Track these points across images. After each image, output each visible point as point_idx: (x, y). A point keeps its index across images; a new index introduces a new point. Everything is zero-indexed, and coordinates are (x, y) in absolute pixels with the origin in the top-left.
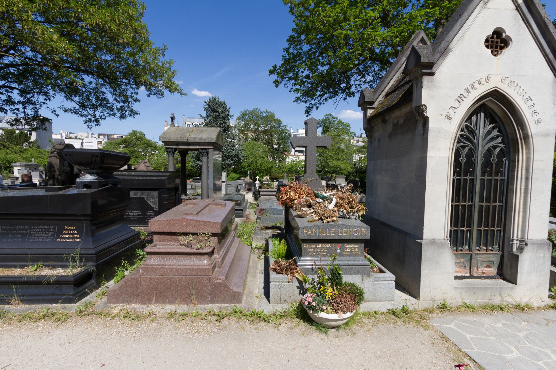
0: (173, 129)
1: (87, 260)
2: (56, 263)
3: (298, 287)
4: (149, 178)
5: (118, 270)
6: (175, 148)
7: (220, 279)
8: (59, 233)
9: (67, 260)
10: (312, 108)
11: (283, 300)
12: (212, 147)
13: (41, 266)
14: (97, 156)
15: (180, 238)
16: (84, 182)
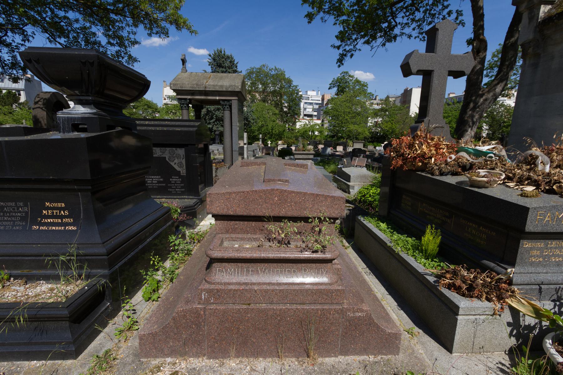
0: (185, 75)
1: (93, 264)
2: (34, 272)
3: (509, 324)
4: (171, 129)
5: (146, 275)
6: (189, 99)
7: (362, 311)
8: (35, 216)
9: (53, 267)
10: (345, 55)
11: (477, 347)
12: (236, 98)
13: (6, 277)
14: (92, 64)
15: (272, 226)
16: (71, 118)
